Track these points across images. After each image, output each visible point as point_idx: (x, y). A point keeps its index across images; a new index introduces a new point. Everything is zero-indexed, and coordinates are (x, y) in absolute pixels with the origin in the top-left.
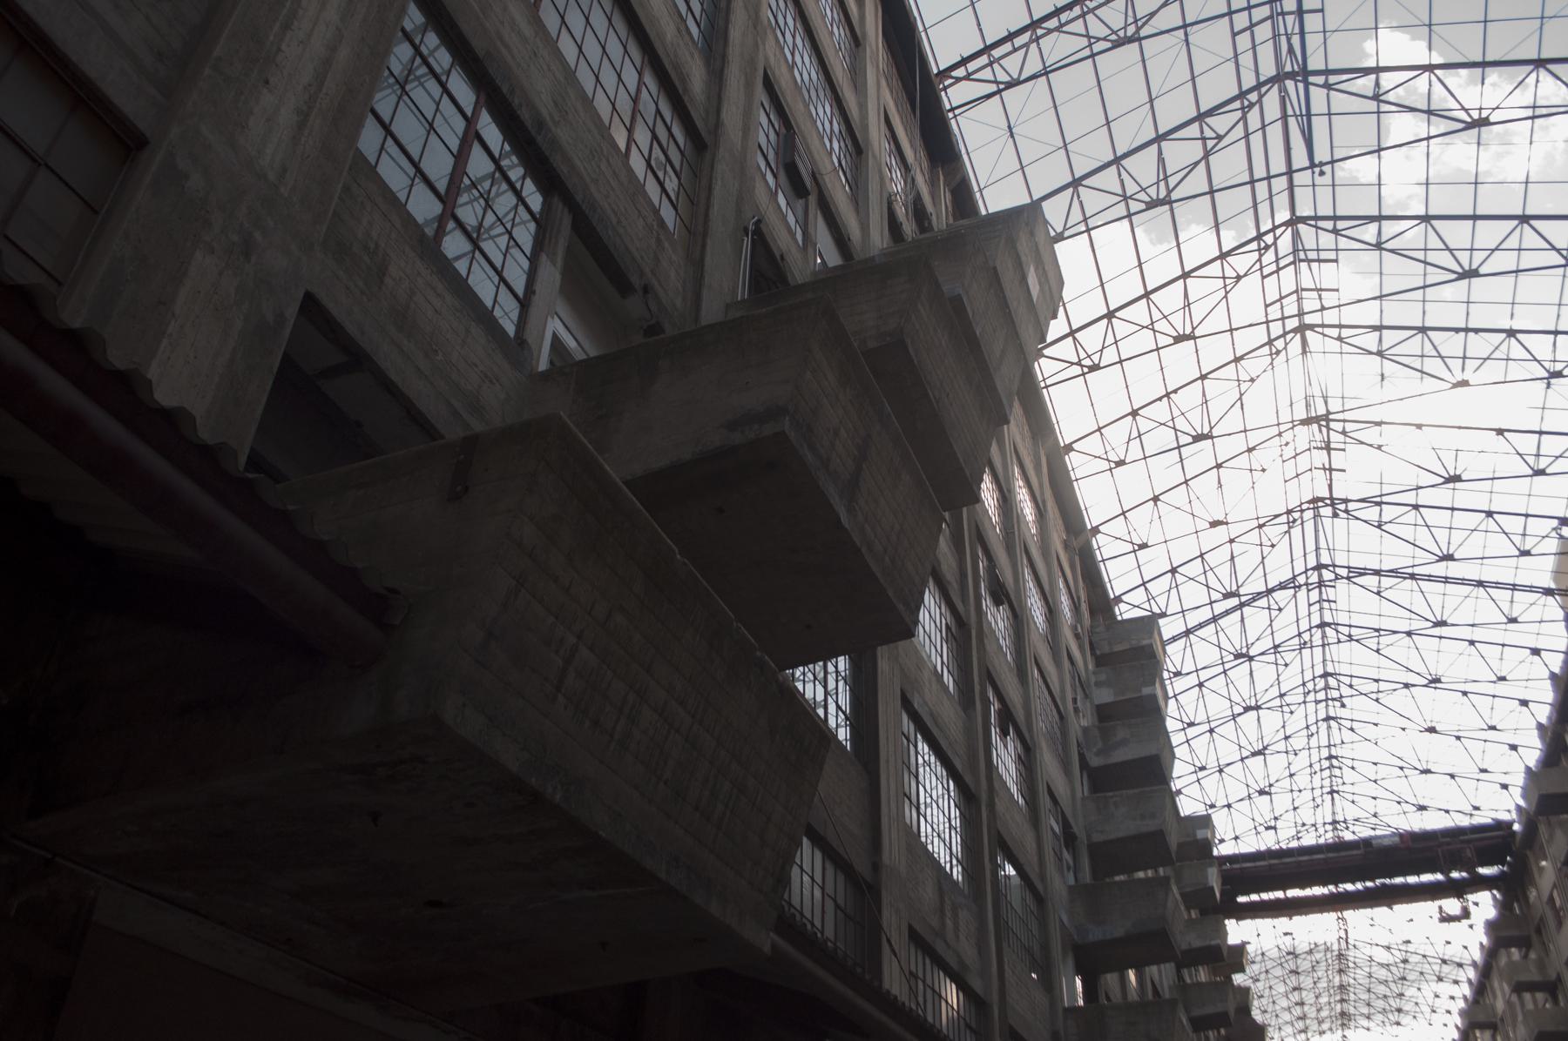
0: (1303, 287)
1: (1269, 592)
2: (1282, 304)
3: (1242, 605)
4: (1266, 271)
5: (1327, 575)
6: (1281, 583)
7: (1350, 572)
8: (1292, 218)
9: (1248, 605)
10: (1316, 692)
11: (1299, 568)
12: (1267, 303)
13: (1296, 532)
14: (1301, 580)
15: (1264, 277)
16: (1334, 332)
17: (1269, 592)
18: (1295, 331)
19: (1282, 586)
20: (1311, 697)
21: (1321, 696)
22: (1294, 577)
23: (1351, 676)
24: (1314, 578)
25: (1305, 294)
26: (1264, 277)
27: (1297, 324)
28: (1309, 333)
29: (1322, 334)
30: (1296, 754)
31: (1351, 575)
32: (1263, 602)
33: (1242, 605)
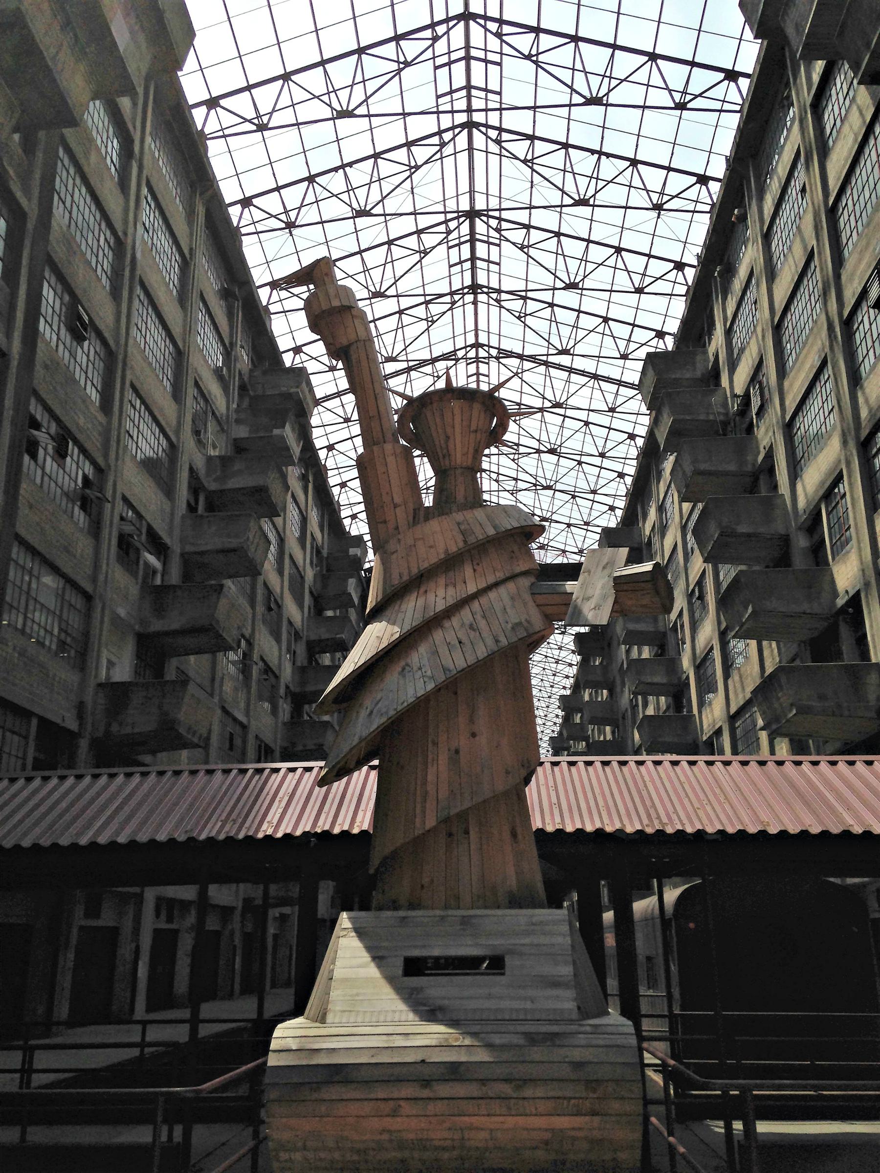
1: (434, 361)
3: (409, 370)
5: (482, 353)
6: (443, 355)
9: (414, 370)
11: (460, 343)
12: (439, 93)
13: (458, 312)
14: (460, 354)
17: (434, 361)
18: (463, 126)
19: (445, 357)
24: (472, 354)
27: (466, 120)
32: (428, 369)
33: (409, 370)
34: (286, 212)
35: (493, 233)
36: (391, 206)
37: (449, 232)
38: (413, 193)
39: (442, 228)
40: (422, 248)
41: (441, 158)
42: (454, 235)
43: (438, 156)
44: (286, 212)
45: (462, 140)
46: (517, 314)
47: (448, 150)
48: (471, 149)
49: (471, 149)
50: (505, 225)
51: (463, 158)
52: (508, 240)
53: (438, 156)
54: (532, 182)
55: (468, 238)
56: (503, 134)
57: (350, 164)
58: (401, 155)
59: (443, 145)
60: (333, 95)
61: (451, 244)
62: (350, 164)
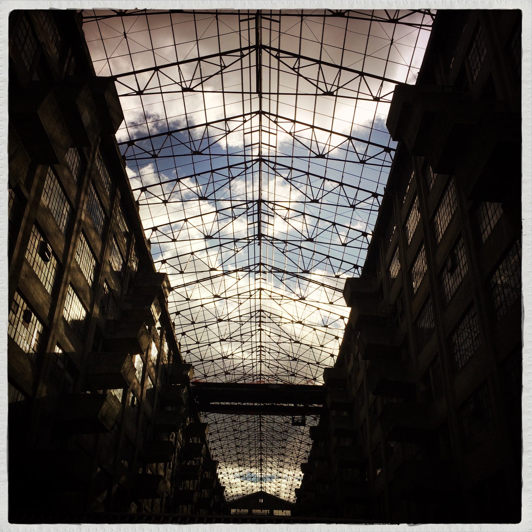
0: (262, 142)
2: (252, 147)
4: (246, 131)
7: (272, 269)
8: (260, 110)
10: (256, 318)
15: (244, 134)
16: (272, 165)
18: (257, 160)
20: (253, 319)
21: (258, 320)
22: (249, 266)
23: (271, 313)
25: (263, 145)
26: (244, 134)
28: (263, 163)
29: (268, 165)
30: (243, 343)
31: (273, 270)
34: (154, 150)
35: (270, 210)
36: (218, 195)
37: (248, 209)
38: (230, 189)
39: (245, 206)
40: (234, 215)
41: (246, 174)
42: (251, 210)
43: (244, 173)
44: (154, 150)
45: (256, 167)
46: (282, 251)
47: (250, 170)
48: (260, 171)
49: (260, 171)
50: (277, 207)
51: (257, 175)
52: (277, 214)
53: (244, 173)
54: (291, 188)
55: (257, 212)
56: (277, 165)
57: (199, 174)
58: (225, 172)
59: (246, 168)
60: (192, 143)
61: (248, 214)
62: (199, 174)
